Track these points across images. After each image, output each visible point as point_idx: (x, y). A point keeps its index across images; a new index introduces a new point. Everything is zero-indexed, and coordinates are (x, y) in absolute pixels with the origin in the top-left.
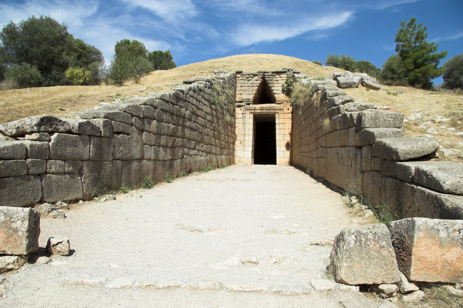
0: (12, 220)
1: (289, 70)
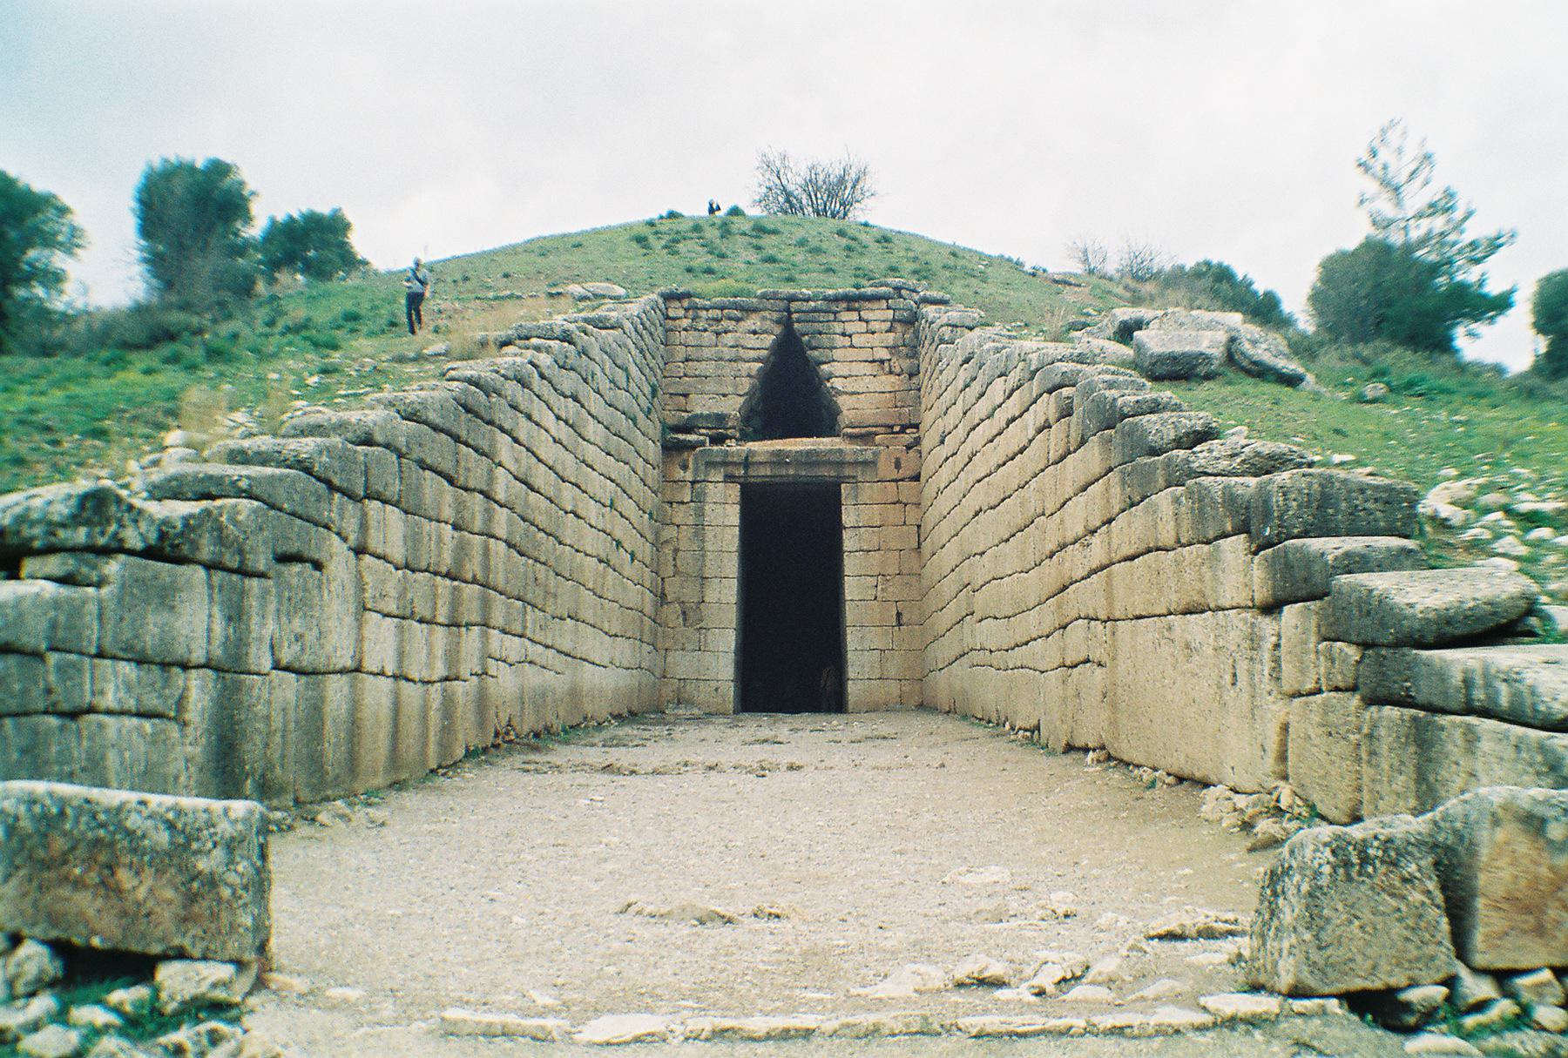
0: (195, 846)
1: (898, 289)
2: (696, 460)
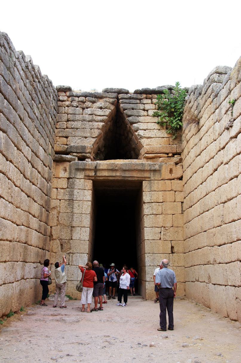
2: (70, 166)
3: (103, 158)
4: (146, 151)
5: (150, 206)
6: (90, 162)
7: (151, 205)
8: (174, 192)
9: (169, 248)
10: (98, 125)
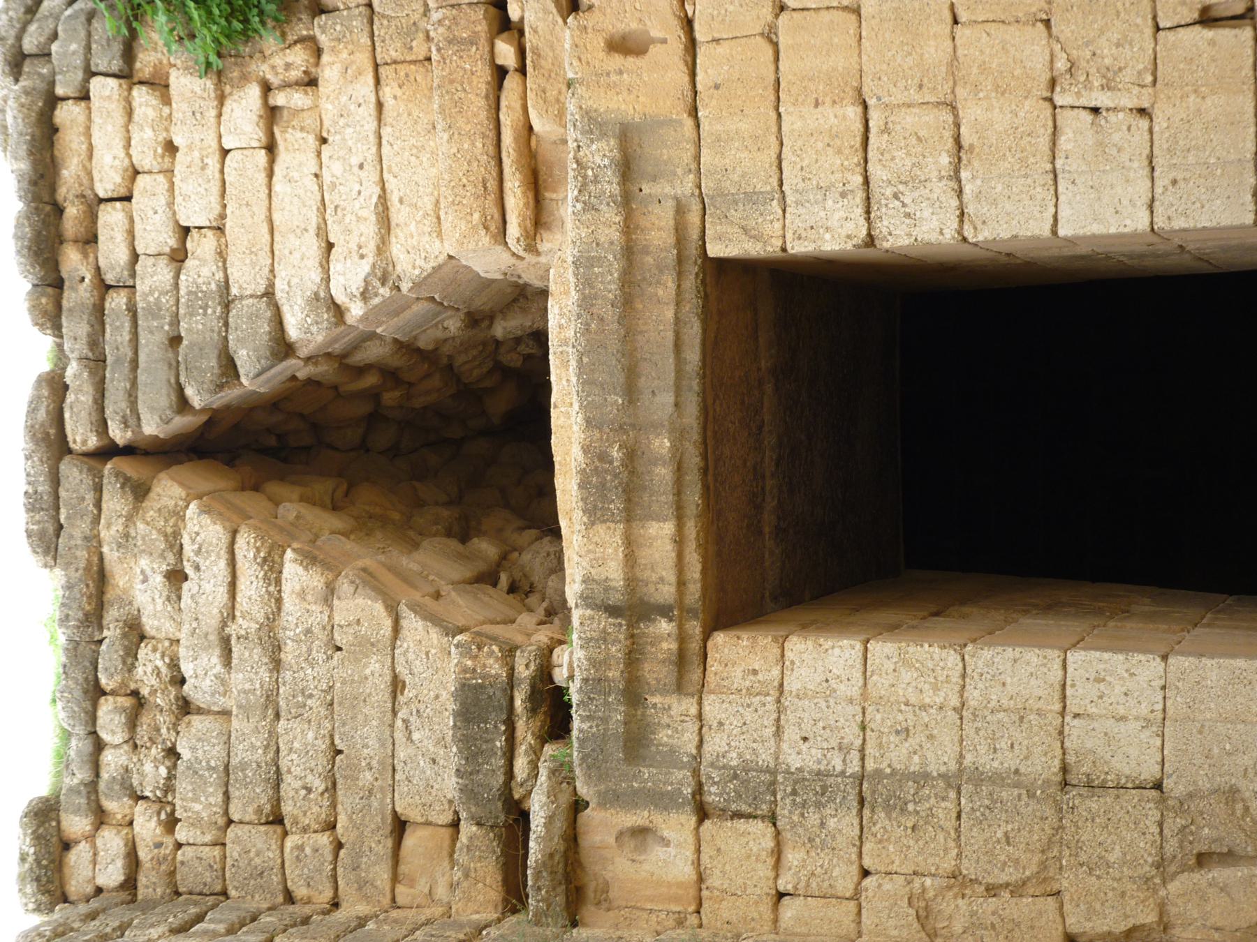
2: (612, 799)
3: (546, 544)
4: (486, 240)
5: (896, 196)
6: (579, 654)
7: (889, 192)
8: (784, 17)
9: (1212, 43)
10: (302, 595)
